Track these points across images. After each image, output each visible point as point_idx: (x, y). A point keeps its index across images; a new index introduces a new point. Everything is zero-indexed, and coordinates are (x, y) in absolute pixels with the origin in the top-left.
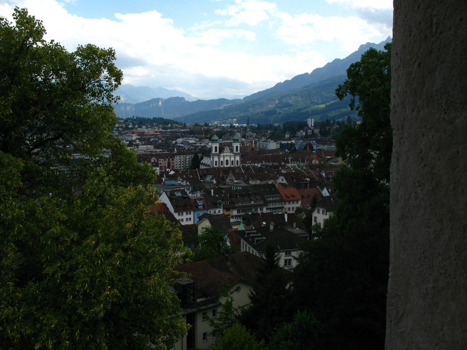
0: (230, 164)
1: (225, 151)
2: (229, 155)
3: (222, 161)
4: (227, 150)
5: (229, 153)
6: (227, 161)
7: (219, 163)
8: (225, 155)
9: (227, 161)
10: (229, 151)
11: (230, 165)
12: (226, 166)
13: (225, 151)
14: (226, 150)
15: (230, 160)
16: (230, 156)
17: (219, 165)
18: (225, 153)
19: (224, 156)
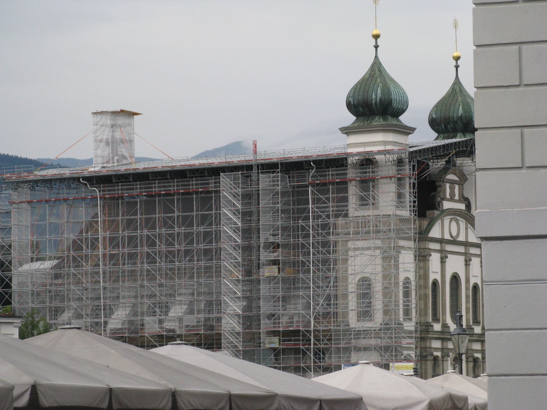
3: (435, 283)
7: (422, 298)
9: (455, 278)
13: (447, 205)
15: (467, 281)
16: (466, 244)
17: (422, 312)
19: (441, 241)
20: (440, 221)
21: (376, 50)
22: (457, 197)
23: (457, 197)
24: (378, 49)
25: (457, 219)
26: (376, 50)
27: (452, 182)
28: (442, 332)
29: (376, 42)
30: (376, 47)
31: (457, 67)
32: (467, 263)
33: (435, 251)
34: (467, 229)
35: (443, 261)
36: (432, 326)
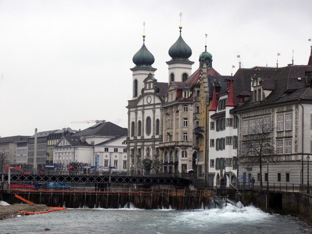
0: (154, 129)
1: (145, 92)
2: (152, 103)
3: (140, 122)
4: (150, 89)
5: (152, 97)
6: (149, 118)
8: (146, 103)
9: (149, 118)
10: (153, 91)
11: (154, 134)
12: (146, 137)
14: (148, 88)
15: (154, 118)
16: (154, 105)
18: (145, 98)
19: (144, 106)
20: (142, 99)
21: (144, 41)
22: (152, 88)
23: (152, 88)
24: (145, 41)
25: (150, 96)
26: (144, 41)
27: (150, 83)
28: (141, 139)
29: (144, 39)
30: (144, 40)
31: (180, 31)
32: (154, 112)
33: (140, 110)
34: (154, 98)
35: (143, 113)
36: (137, 138)
